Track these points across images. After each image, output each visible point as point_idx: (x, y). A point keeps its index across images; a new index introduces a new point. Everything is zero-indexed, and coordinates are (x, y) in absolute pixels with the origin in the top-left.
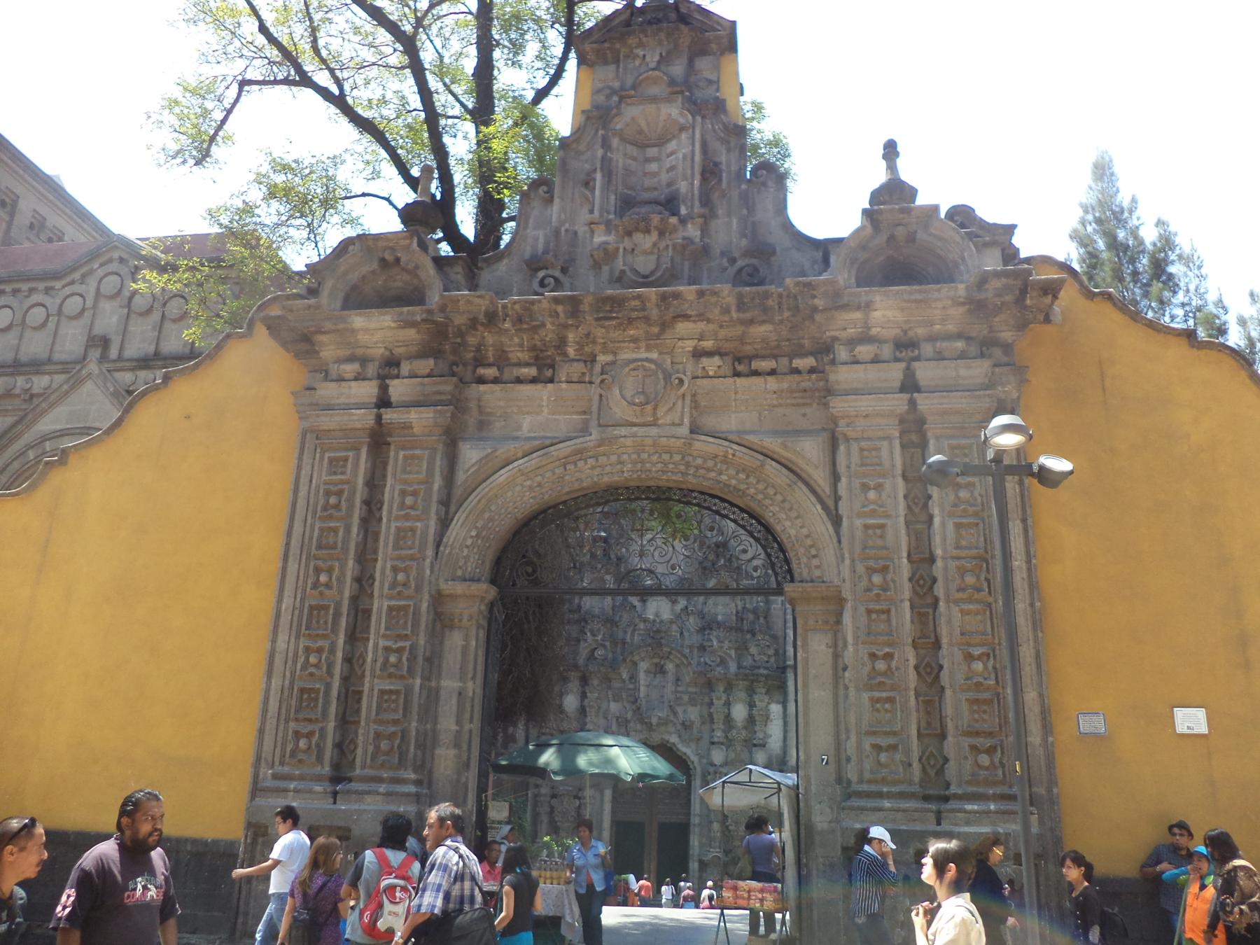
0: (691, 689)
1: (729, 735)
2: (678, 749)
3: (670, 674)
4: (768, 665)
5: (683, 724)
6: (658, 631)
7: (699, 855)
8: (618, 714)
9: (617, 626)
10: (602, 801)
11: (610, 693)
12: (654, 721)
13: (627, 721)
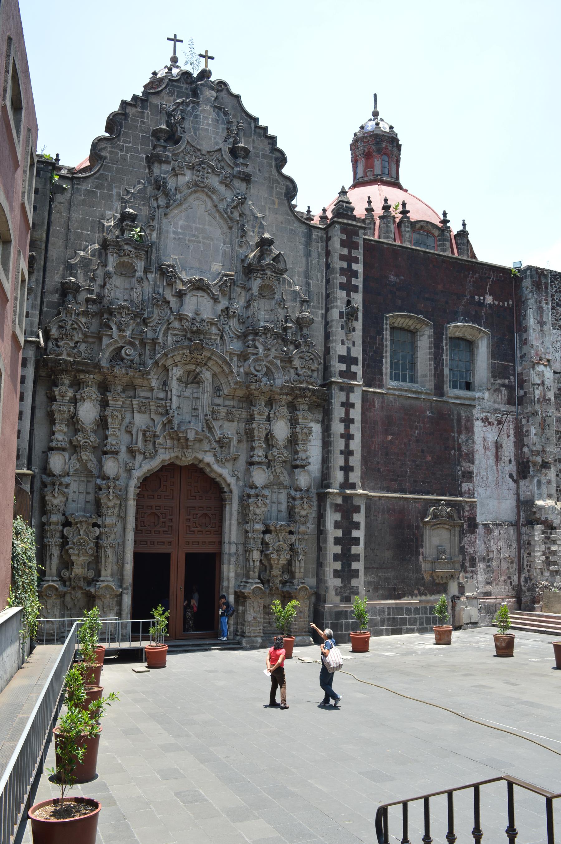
0: (231, 403)
2: (212, 470)
4: (312, 380)
5: (219, 442)
6: (198, 332)
8: (144, 427)
10: (124, 529)
11: (135, 402)
12: (191, 435)
13: (155, 436)
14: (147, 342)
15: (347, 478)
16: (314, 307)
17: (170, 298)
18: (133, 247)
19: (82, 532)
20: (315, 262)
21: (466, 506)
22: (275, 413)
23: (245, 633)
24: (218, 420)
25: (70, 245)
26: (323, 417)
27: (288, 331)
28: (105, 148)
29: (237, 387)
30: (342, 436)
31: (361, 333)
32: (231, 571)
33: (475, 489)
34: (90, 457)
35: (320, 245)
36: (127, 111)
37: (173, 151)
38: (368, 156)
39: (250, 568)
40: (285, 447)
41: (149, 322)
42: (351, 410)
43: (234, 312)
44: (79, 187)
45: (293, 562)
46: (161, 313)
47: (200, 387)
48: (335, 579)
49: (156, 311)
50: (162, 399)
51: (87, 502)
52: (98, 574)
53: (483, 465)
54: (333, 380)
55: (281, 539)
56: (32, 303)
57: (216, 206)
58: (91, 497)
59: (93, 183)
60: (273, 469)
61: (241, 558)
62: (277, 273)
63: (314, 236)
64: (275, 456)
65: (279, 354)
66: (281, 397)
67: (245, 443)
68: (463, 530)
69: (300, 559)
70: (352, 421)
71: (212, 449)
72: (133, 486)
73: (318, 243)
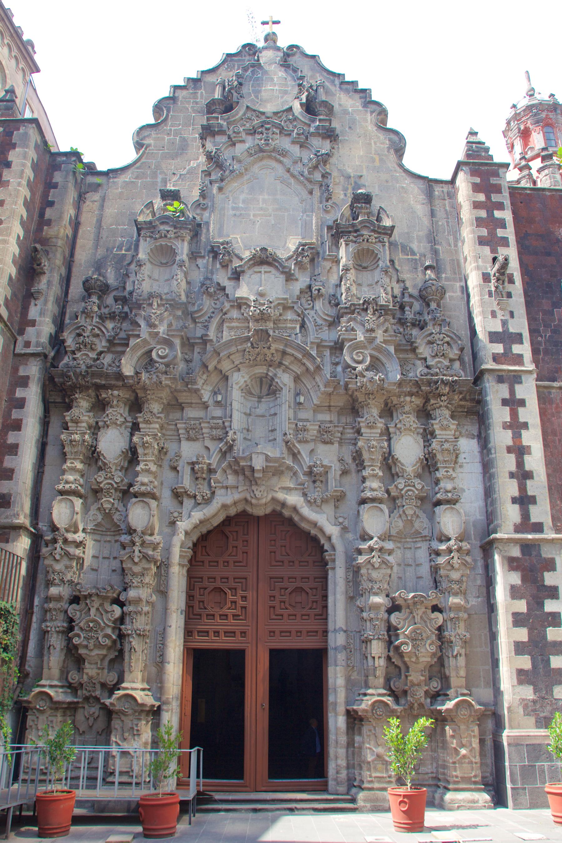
0: (326, 417)
1: (391, 488)
2: (303, 518)
3: (285, 391)
5: (310, 473)
6: (262, 317)
7: (347, 703)
8: (194, 460)
9: (194, 321)
12: (258, 463)
13: (211, 471)
14: (196, 343)
15: (525, 516)
16: (447, 279)
17: (225, 282)
18: (171, 226)
19: (93, 611)
20: (443, 224)
22: (396, 425)
23: (363, 782)
24: (306, 442)
25: (101, 242)
26: (480, 428)
27: (407, 308)
28: (148, 136)
29: (330, 390)
30: (509, 450)
31: (523, 300)
32: (339, 675)
34: (116, 506)
35: (447, 202)
36: (176, 95)
37: (229, 118)
38: (525, 135)
39: (368, 670)
40: (419, 476)
41: (199, 317)
42: (521, 410)
43: (319, 290)
44: (115, 180)
45: (446, 659)
46: (216, 304)
47: (276, 398)
48: (521, 687)
49: (207, 304)
50: (220, 418)
51: (114, 571)
52: (121, 679)
54: (483, 367)
55: (418, 619)
56: (41, 309)
57: (288, 171)
58: (115, 564)
59: (132, 173)
60: (401, 510)
61: (358, 656)
62: (379, 233)
63: (436, 193)
64: (402, 490)
65: (391, 336)
66: (402, 399)
67: (354, 474)
69: (455, 653)
70: (525, 425)
71: (299, 485)
72: (179, 544)
73: (444, 200)
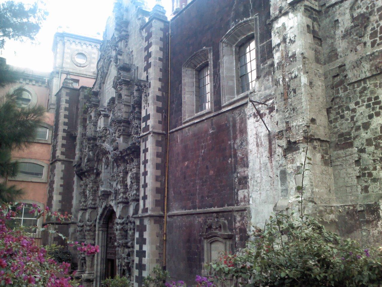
21: (238, 216)
33: (250, 195)
53: (257, 167)
68: (236, 243)
